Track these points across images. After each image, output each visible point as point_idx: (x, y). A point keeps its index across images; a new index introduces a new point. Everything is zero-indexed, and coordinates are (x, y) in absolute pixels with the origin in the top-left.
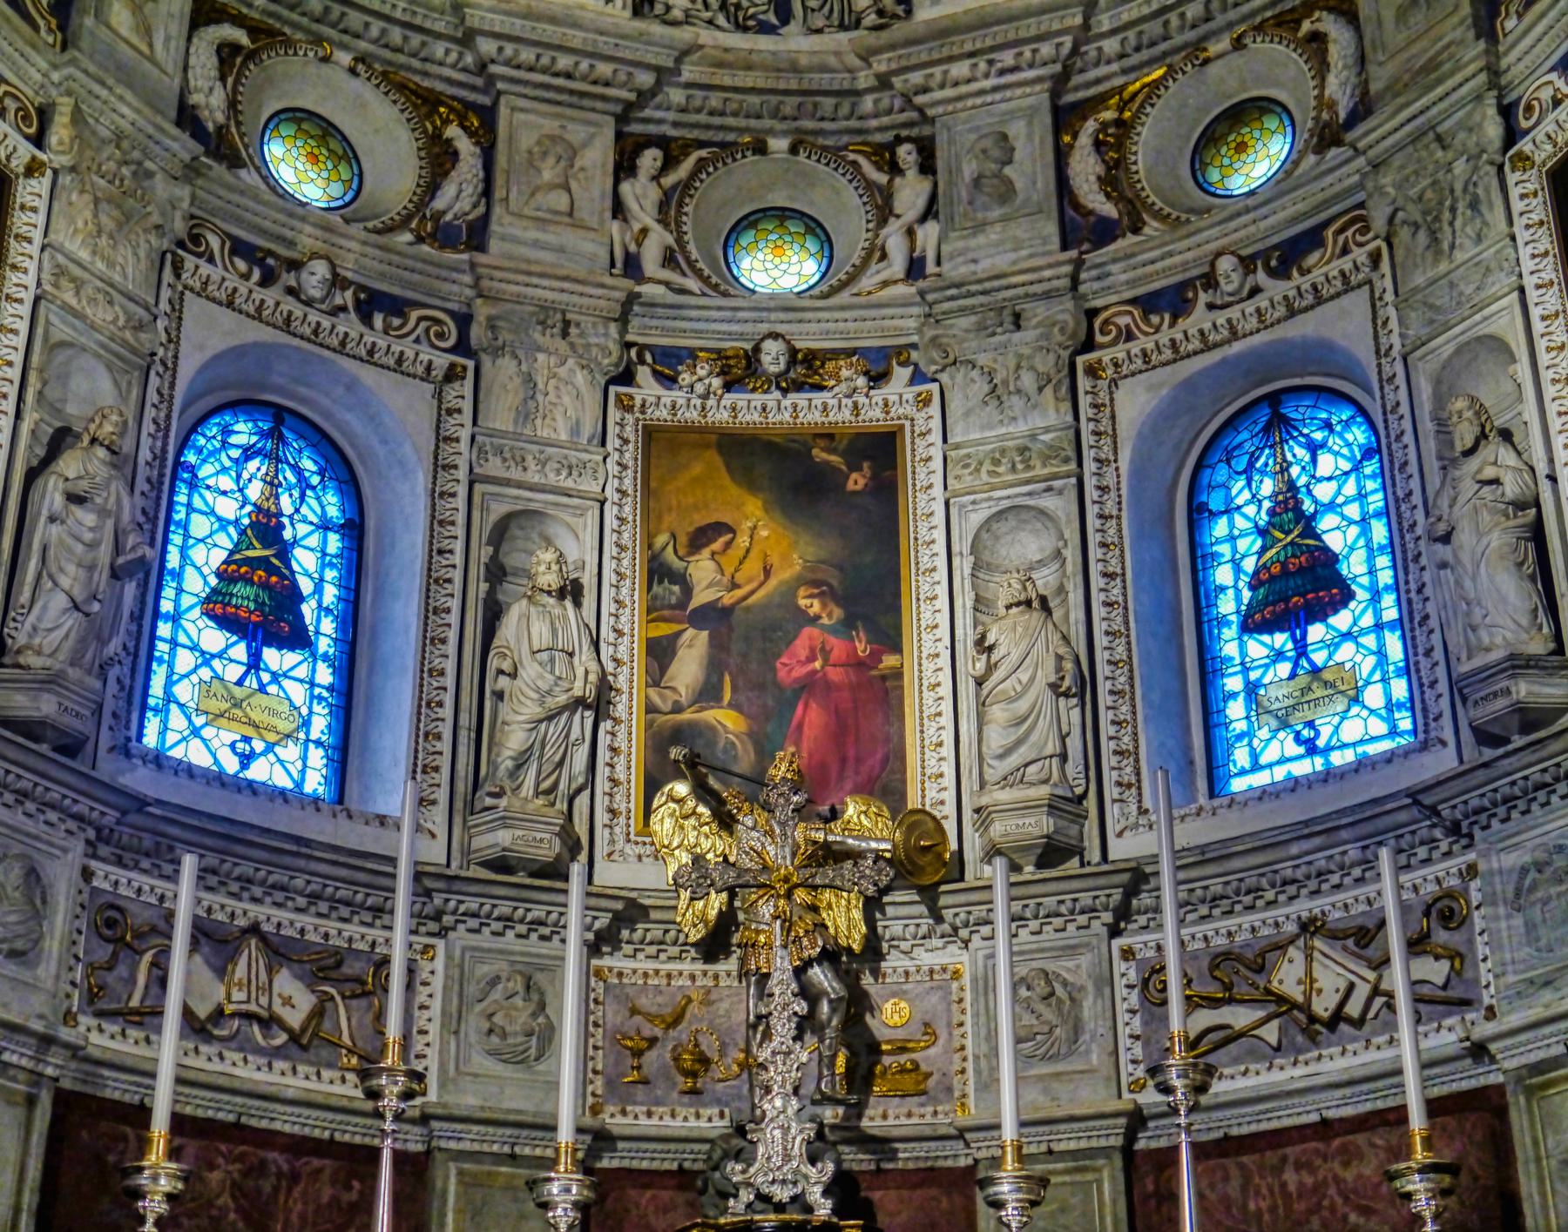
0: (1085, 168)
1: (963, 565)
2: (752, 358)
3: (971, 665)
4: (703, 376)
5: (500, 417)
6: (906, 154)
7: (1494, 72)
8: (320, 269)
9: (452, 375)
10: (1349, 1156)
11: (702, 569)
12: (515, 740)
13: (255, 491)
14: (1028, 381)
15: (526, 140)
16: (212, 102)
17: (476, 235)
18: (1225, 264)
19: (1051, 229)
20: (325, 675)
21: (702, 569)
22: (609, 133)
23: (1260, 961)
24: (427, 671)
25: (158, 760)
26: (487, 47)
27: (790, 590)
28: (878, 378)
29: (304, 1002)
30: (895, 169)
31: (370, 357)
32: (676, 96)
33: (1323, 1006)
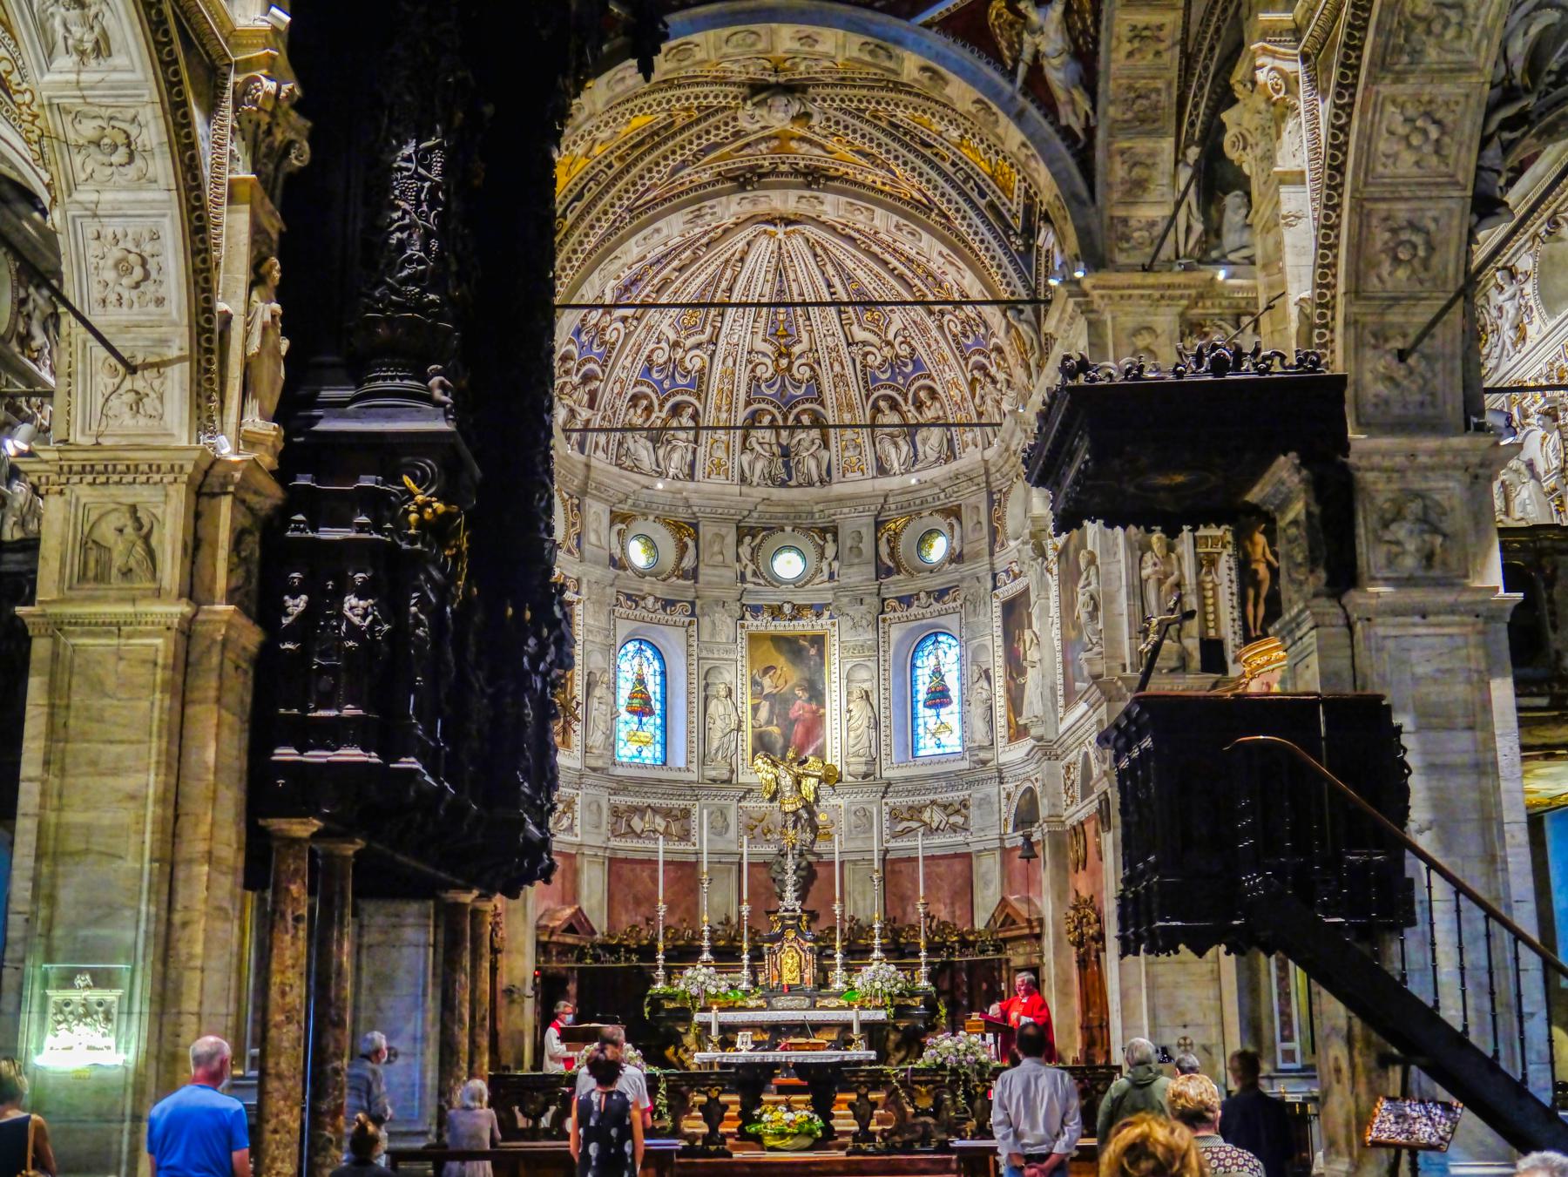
0: (884, 550)
1: (844, 682)
2: (780, 608)
3: (846, 716)
4: (766, 616)
5: (705, 637)
6: (829, 536)
7: (992, 564)
8: (650, 600)
9: (690, 623)
10: (938, 865)
11: (767, 682)
12: (715, 744)
13: (636, 668)
14: (864, 623)
15: (709, 536)
16: (617, 552)
17: (693, 574)
18: (922, 595)
19: (872, 569)
20: (659, 721)
21: (767, 682)
22: (734, 530)
23: (920, 810)
24: (689, 722)
25: (622, 764)
26: (696, 509)
27: (793, 689)
28: (819, 615)
29: (663, 824)
30: (825, 540)
31: (667, 624)
32: (755, 515)
33: (934, 825)
